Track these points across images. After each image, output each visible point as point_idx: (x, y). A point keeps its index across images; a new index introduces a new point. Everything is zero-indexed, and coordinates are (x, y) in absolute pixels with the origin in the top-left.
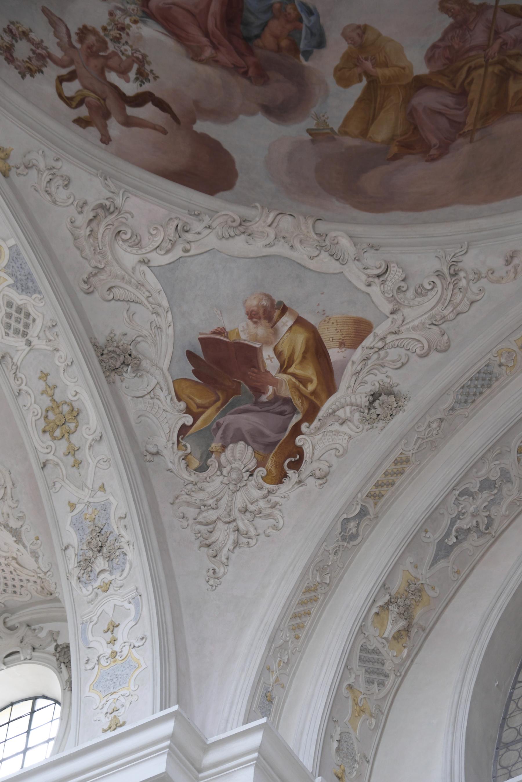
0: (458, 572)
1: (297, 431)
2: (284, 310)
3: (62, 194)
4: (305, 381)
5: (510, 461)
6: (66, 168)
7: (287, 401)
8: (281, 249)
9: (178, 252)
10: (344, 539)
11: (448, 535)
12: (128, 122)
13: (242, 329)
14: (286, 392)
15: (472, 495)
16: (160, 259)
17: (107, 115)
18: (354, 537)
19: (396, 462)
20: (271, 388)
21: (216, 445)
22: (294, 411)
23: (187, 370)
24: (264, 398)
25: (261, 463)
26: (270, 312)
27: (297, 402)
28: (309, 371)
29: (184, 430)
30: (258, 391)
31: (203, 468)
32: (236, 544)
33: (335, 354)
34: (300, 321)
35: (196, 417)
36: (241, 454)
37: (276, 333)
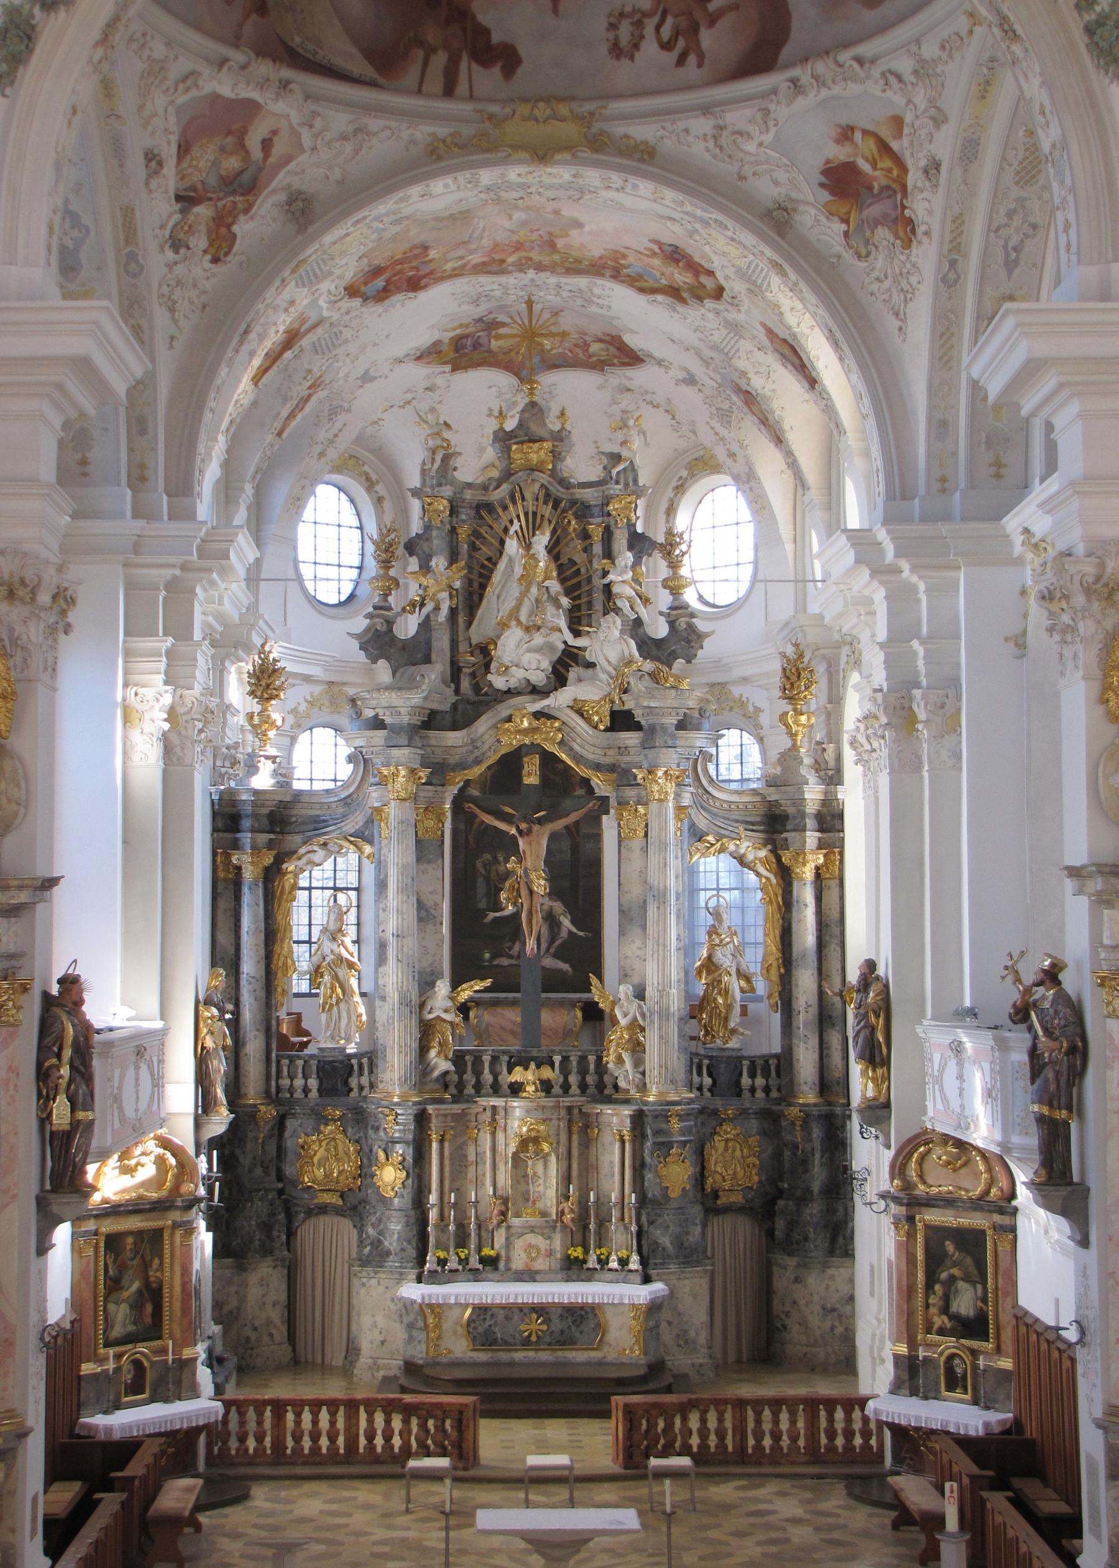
0: (1034, 265)
1: (904, 207)
2: (852, 129)
3: (690, 139)
4: (889, 170)
5: (1016, 192)
6: (682, 125)
7: (888, 187)
8: (824, 93)
9: (773, 130)
10: (950, 287)
11: (1007, 255)
12: (713, 19)
13: (840, 154)
14: (884, 182)
15: (1007, 225)
16: (768, 138)
17: (695, 29)
18: (956, 281)
19: (954, 221)
20: (875, 184)
21: (868, 234)
22: (895, 192)
23: (825, 196)
24: (876, 191)
25: (897, 237)
26: (846, 134)
27: (894, 186)
28: (888, 163)
29: (846, 234)
30: (870, 188)
31: (869, 254)
32: (906, 301)
33: (895, 145)
34: (865, 132)
35: (846, 221)
36: (883, 234)
37: (856, 146)
